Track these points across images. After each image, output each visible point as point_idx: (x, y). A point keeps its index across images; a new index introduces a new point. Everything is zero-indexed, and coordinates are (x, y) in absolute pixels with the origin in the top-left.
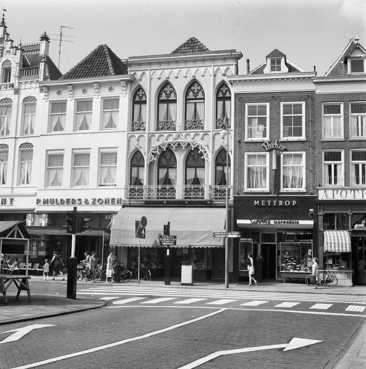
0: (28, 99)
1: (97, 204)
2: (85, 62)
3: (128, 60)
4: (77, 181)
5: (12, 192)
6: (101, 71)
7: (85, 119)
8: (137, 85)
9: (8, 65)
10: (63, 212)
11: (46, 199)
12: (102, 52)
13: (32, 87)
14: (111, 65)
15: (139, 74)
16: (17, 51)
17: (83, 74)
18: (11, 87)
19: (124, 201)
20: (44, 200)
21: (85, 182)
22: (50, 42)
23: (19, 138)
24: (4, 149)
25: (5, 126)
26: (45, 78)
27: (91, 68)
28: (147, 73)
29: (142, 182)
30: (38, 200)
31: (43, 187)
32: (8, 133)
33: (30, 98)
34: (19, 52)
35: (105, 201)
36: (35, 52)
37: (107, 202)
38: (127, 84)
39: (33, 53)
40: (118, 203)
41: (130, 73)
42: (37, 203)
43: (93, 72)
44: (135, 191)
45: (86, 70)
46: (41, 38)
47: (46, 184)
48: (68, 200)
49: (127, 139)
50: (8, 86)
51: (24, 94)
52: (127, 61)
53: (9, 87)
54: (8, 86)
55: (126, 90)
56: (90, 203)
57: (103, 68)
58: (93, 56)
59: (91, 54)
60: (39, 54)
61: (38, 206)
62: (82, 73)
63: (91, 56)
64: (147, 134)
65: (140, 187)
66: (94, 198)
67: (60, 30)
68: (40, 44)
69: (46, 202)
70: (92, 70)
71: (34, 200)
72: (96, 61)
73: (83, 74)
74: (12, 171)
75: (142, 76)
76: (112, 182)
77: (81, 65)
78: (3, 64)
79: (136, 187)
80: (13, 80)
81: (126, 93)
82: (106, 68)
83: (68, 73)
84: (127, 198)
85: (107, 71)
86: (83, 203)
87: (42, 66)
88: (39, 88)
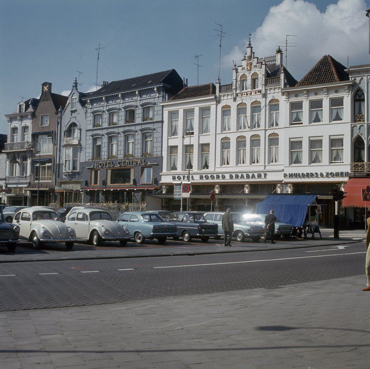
0: (273, 101)
1: (330, 176)
2: (314, 70)
3: (350, 70)
4: (313, 160)
5: (265, 169)
6: (328, 78)
7: (317, 115)
8: (357, 87)
9: (255, 76)
10: (304, 183)
11: (291, 173)
12: (327, 62)
13: (275, 91)
14: (335, 73)
15: (358, 80)
16: (262, 66)
17: (314, 81)
18: (259, 93)
19: (350, 174)
20: (289, 174)
21: (320, 160)
22: (283, 54)
23: (268, 130)
24: (256, 138)
25: (256, 121)
26: (285, 85)
27: (320, 76)
28: (365, 78)
29: (363, 160)
30: (284, 174)
31: (288, 165)
32: (259, 126)
33: (274, 100)
34: (264, 66)
35: (336, 173)
36: (272, 63)
37: (337, 175)
38: (349, 88)
39: (270, 63)
40: (346, 175)
41: (351, 79)
42: (285, 176)
43: (321, 79)
44: (359, 167)
45: (316, 77)
46: (277, 51)
47: (291, 163)
48: (308, 174)
49: (351, 128)
50: (257, 92)
51: (269, 98)
52: (349, 70)
53: (258, 92)
54: (257, 92)
55: (349, 92)
56: (324, 176)
57: (329, 75)
58: (320, 65)
59: (318, 63)
60: (275, 64)
61: (285, 179)
62: (313, 80)
63: (318, 66)
64: (366, 124)
65: (361, 163)
66: (327, 172)
67: (286, 38)
68: (276, 56)
69: (291, 176)
70: (320, 76)
71: (282, 173)
72: (323, 69)
73: (314, 81)
74: (264, 154)
75: (360, 81)
76: (340, 160)
77: (311, 73)
78: (252, 75)
79: (359, 163)
80: (260, 86)
81: (349, 94)
82: (331, 75)
83: (302, 80)
84: (353, 172)
85: (333, 77)
86: (319, 176)
87: (282, 76)
88: (281, 92)
